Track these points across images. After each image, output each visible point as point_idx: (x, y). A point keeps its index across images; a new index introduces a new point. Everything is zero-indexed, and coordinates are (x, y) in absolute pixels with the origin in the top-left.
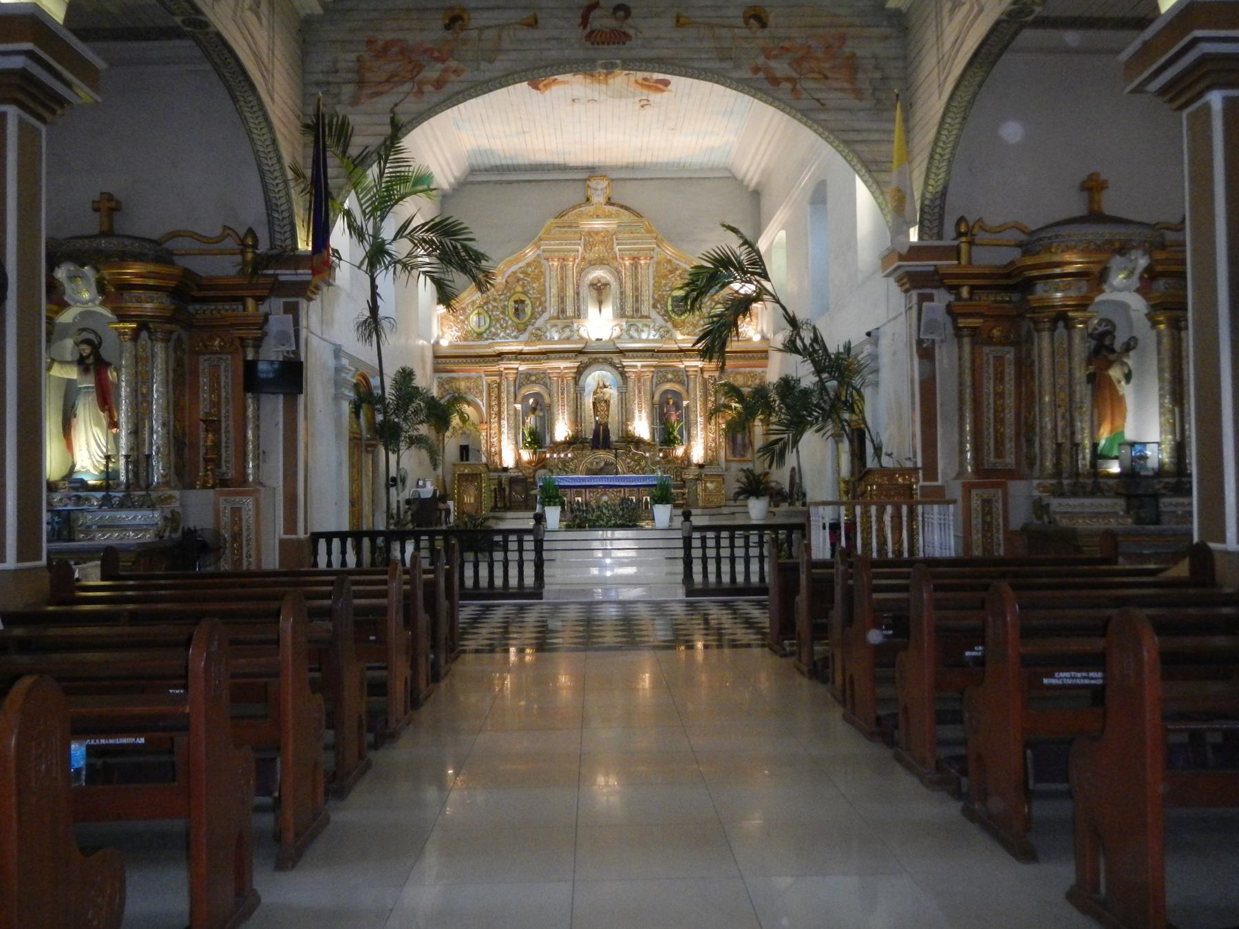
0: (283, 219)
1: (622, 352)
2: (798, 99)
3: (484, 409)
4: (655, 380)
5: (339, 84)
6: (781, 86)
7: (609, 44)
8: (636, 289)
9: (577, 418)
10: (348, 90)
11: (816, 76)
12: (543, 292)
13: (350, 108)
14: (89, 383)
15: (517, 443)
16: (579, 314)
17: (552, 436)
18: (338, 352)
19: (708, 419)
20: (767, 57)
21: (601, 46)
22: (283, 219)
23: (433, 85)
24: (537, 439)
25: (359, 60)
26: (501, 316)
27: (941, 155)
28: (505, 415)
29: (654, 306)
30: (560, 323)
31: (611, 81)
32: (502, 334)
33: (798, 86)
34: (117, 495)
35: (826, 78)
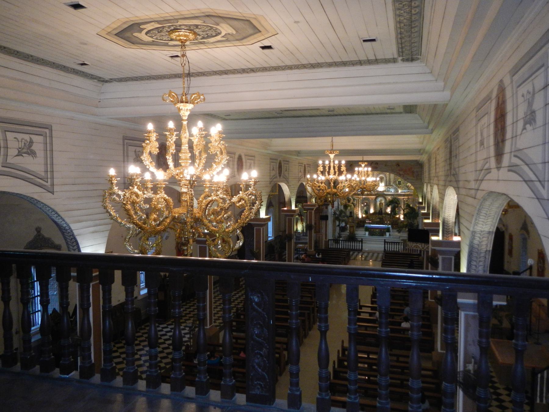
6: (402, 175)
8: (390, 179)
14: (300, 218)
15: (362, 212)
17: (370, 212)
24: (367, 212)
28: (359, 207)
34: (305, 234)
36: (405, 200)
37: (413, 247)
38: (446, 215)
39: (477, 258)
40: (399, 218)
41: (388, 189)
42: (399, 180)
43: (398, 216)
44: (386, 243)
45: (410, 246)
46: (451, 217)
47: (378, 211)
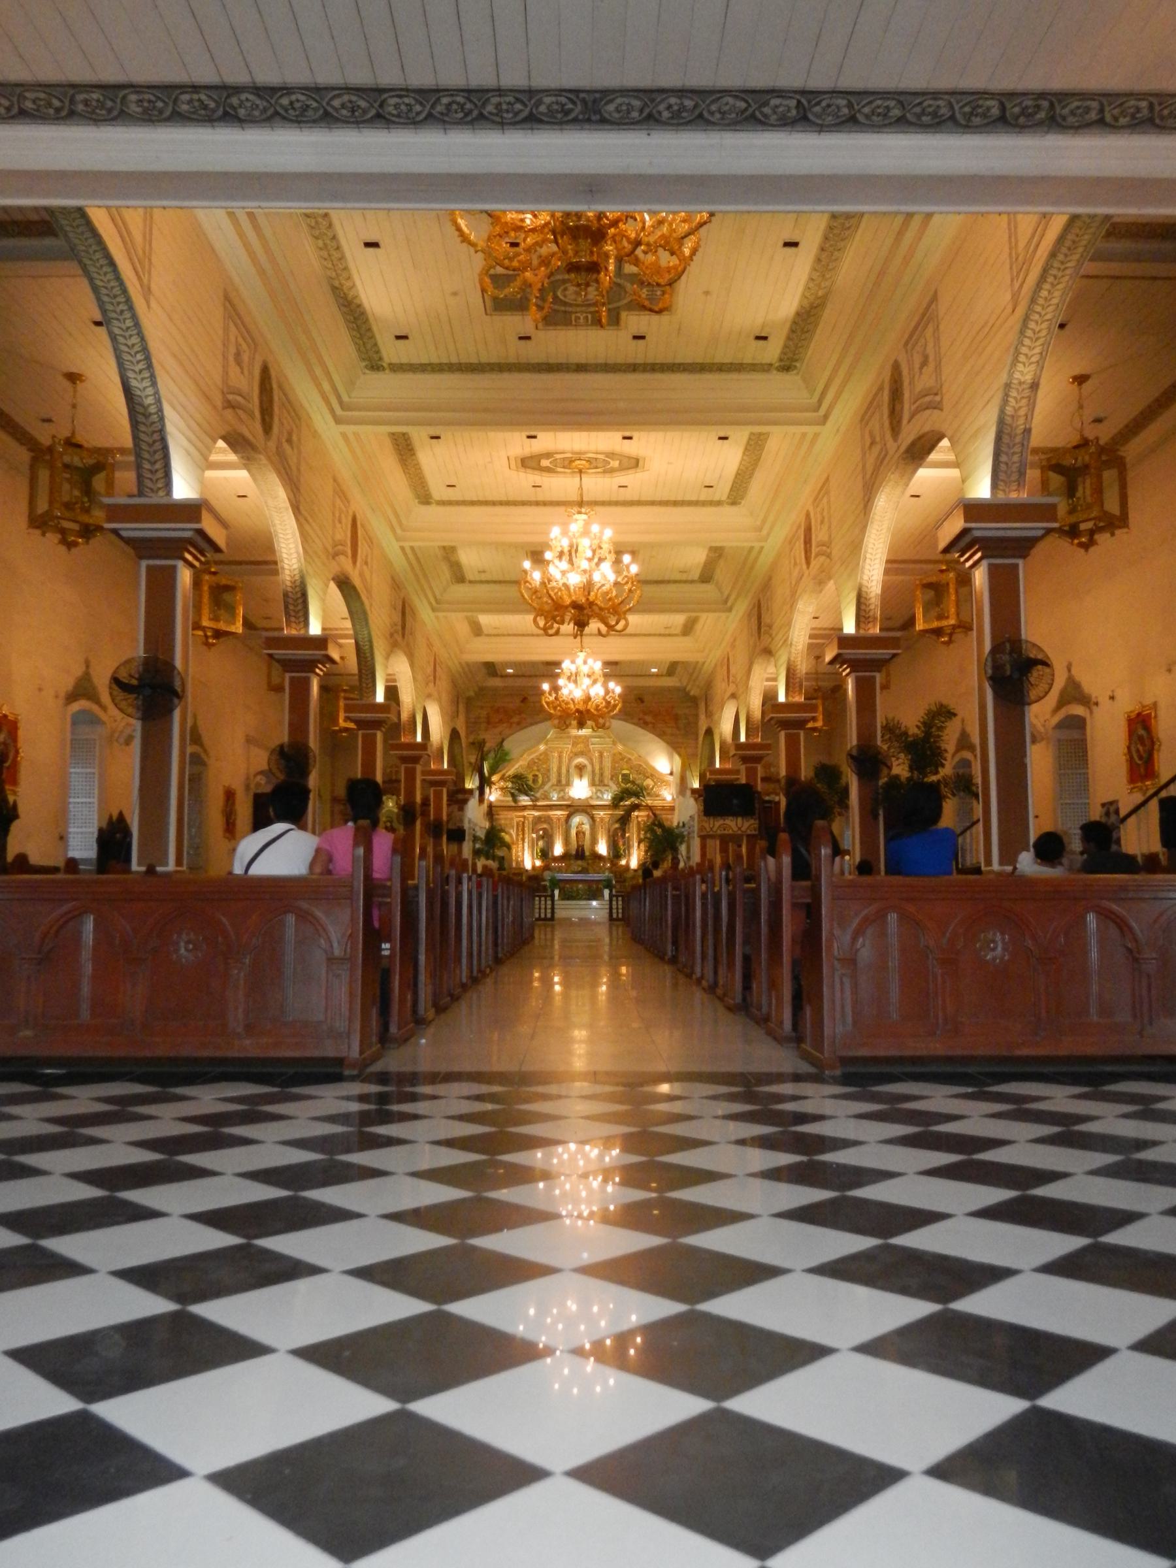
1: (593, 807)
3: (514, 836)
6: (650, 725)
8: (601, 769)
9: (567, 842)
10: (483, 726)
12: (548, 770)
16: (569, 784)
17: (552, 852)
18: (470, 821)
19: (639, 843)
24: (545, 854)
25: (488, 714)
28: (526, 840)
29: (612, 779)
30: (558, 788)
36: (640, 819)
37: (715, 829)
38: (865, 578)
39: (1009, 447)
40: (627, 866)
41: (599, 794)
43: (623, 862)
44: (614, 899)
45: (708, 829)
46: (874, 583)
47: (574, 853)
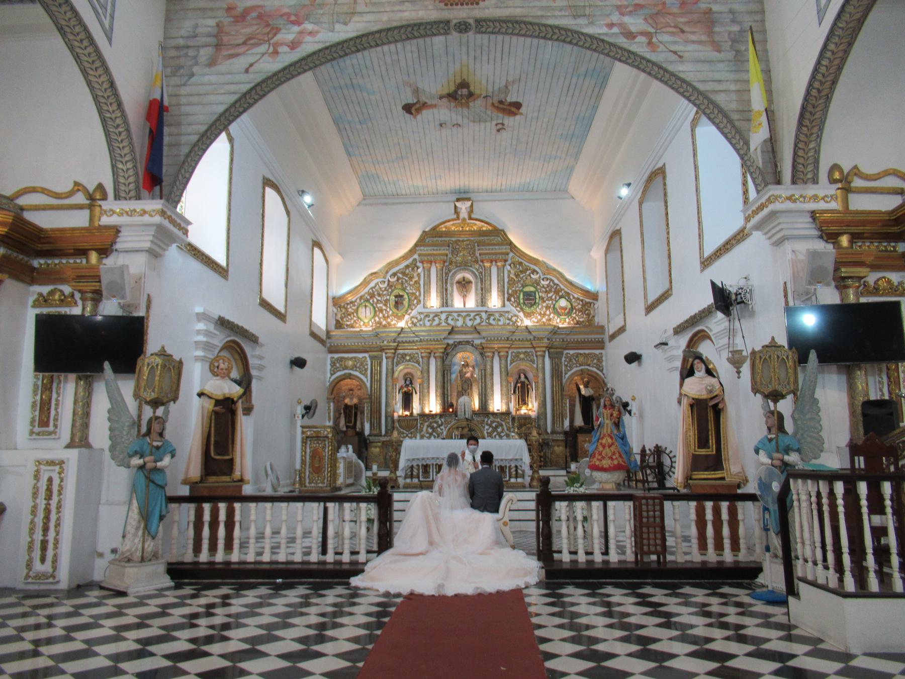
0: (128, 169)
2: (654, 51)
4: (509, 359)
5: (198, 47)
6: (638, 39)
7: (462, 4)
10: (205, 54)
11: (674, 30)
13: (207, 70)
20: (622, 14)
21: (454, 7)
22: (128, 169)
23: (288, 46)
25: (218, 25)
26: (384, 308)
27: (819, 91)
29: (509, 300)
31: (471, 104)
32: (384, 323)
33: (654, 40)
35: (683, 31)
42: (527, 289)
